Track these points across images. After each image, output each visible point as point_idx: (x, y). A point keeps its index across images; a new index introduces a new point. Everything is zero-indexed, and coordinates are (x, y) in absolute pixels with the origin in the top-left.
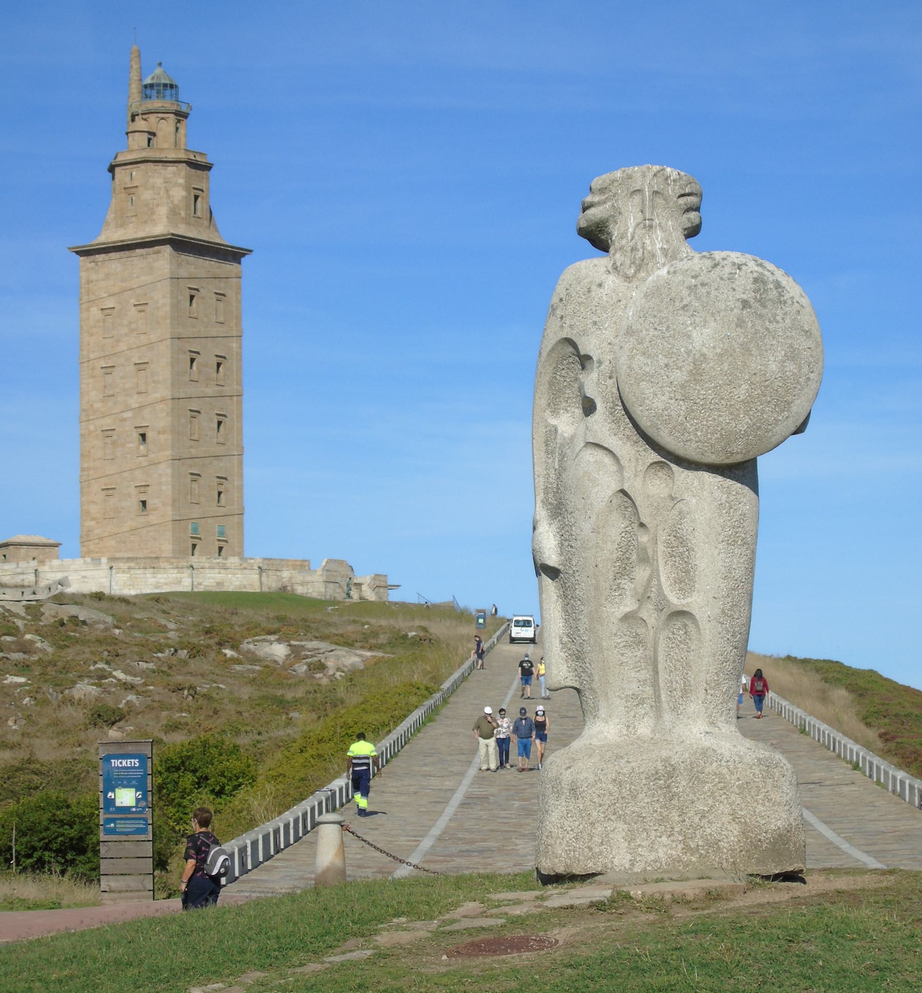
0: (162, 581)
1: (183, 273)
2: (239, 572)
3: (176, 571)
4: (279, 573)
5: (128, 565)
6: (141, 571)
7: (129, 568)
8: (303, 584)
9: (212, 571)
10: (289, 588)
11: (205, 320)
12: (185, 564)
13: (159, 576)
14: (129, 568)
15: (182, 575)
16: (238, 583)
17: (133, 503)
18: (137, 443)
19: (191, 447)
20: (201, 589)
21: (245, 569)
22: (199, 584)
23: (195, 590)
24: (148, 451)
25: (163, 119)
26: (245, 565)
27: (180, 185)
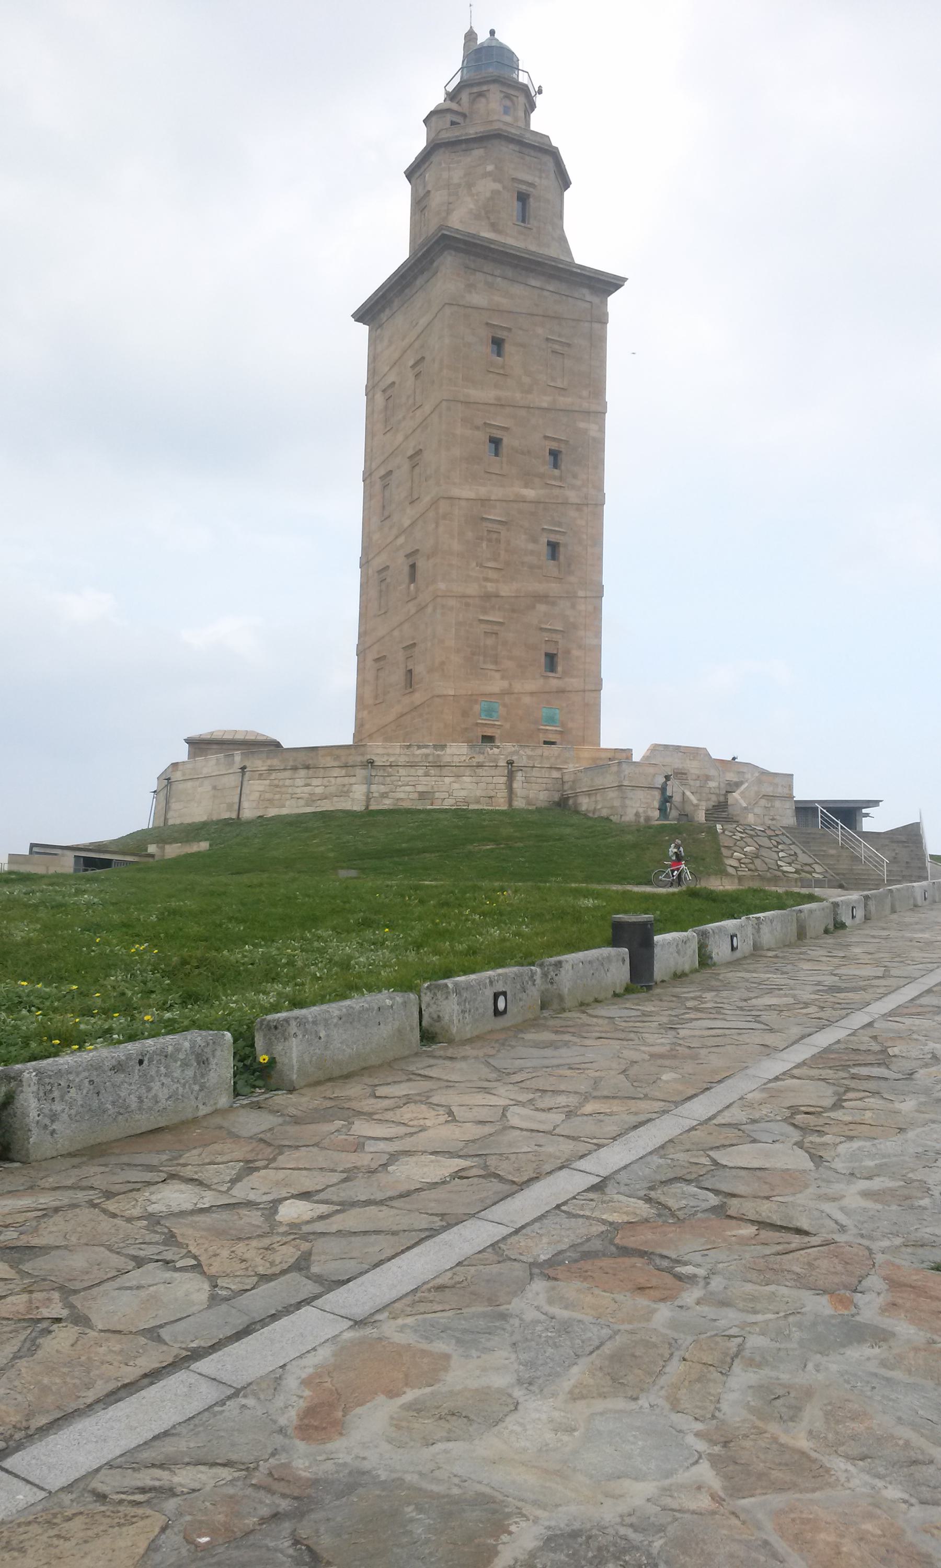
0: (319, 790)
1: (478, 299)
2: (468, 773)
3: (343, 772)
4: (556, 774)
5: (269, 762)
6: (288, 774)
7: (271, 770)
8: (589, 793)
9: (412, 771)
10: (571, 802)
11: (526, 380)
12: (359, 759)
13: (315, 782)
14: (271, 770)
15: (353, 780)
16: (463, 793)
17: (397, 677)
18: (407, 580)
19: (486, 579)
20: (387, 804)
21: (480, 766)
22: (384, 795)
23: (373, 807)
24: (417, 590)
25: (481, 94)
26: (480, 758)
27: (489, 174)
